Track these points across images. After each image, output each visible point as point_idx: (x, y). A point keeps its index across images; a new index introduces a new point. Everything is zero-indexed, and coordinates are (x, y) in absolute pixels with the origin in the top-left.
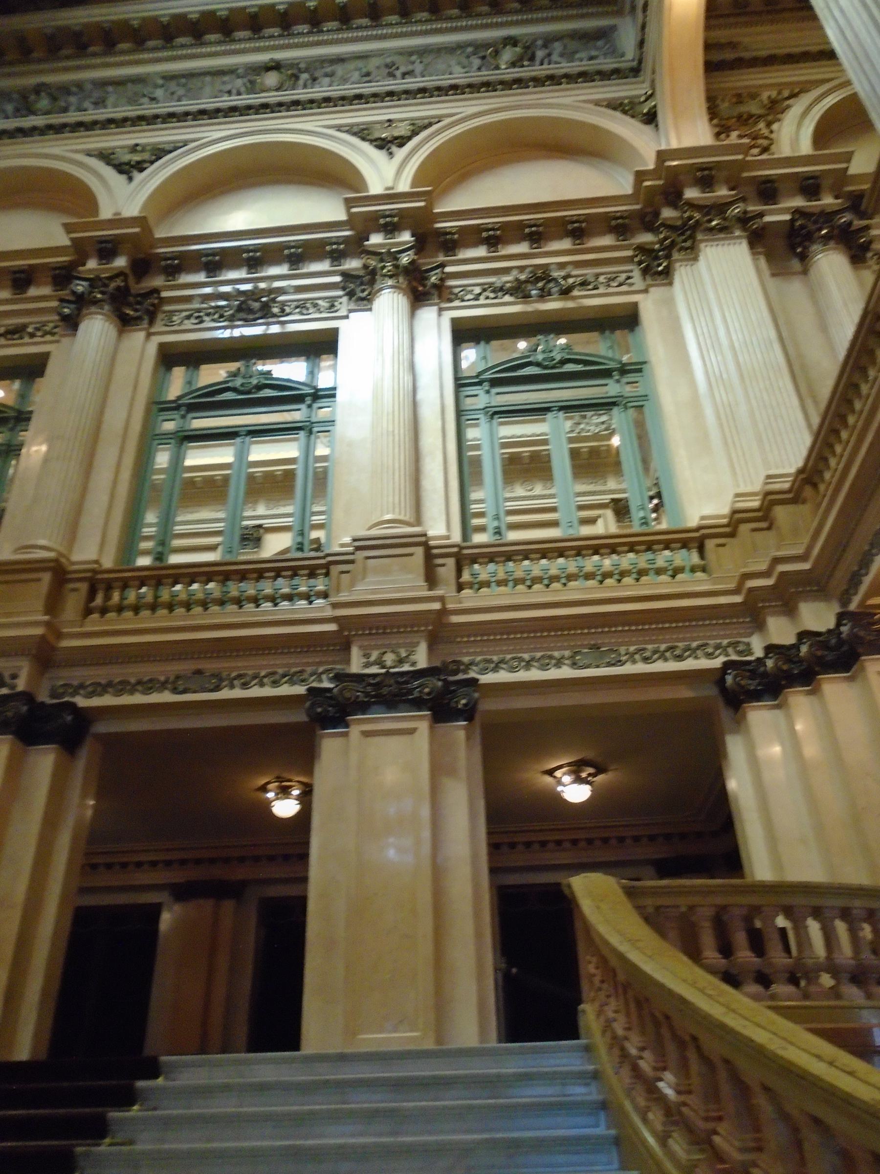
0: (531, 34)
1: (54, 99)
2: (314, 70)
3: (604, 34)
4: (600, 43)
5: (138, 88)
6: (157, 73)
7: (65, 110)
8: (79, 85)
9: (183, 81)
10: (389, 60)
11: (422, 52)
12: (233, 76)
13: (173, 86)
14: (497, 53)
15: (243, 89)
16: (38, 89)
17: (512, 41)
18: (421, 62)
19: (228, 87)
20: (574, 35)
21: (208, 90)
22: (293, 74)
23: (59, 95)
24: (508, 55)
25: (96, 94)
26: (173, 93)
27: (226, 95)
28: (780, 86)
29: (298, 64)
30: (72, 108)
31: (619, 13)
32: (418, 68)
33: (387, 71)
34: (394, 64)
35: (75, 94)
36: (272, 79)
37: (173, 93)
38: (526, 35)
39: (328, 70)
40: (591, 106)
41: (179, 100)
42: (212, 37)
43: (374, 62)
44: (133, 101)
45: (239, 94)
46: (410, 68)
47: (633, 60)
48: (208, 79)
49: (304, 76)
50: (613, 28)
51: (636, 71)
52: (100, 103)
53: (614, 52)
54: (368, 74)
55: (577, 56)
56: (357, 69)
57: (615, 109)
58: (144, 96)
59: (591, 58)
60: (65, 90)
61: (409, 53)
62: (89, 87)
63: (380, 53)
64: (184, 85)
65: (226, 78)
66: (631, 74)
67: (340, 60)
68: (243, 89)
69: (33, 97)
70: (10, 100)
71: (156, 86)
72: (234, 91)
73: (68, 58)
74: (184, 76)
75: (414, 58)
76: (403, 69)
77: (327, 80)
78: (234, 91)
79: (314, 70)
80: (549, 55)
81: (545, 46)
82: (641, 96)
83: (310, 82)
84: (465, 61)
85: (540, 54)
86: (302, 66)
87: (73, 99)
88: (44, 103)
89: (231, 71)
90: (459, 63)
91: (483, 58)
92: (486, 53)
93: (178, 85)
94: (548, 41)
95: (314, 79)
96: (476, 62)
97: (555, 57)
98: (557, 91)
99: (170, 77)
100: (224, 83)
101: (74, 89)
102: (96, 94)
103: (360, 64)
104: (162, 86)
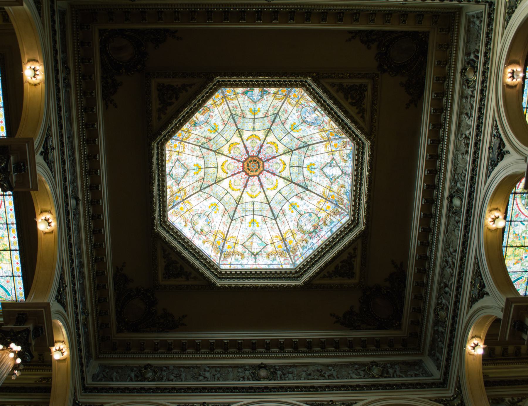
0: (383, 361)
1: (155, 373)
2: (285, 371)
3: (418, 364)
4: (416, 367)
5: (196, 370)
6: (206, 365)
7: (160, 379)
8: (167, 367)
9: (219, 369)
10: (319, 368)
11: (334, 365)
12: (243, 369)
13: (213, 371)
14: (369, 369)
15: (250, 377)
16: (147, 367)
17: (376, 364)
18: (334, 370)
19: (242, 375)
20: (404, 363)
21: (231, 375)
22: (274, 372)
23: (158, 372)
24: (376, 371)
25: (176, 372)
26: (214, 375)
27: (242, 379)
28: (512, 396)
29: (275, 366)
30: (165, 378)
31: (422, 354)
32: (335, 374)
33: (319, 373)
34: (322, 371)
35: (165, 371)
36: (263, 373)
37: (214, 375)
38: (382, 361)
39: (290, 370)
40: (427, 400)
41: (218, 380)
42: (233, 350)
43: (311, 368)
44: (196, 379)
45: (249, 379)
46: (330, 372)
47: (440, 379)
48: (230, 369)
49: (279, 373)
50: (421, 361)
51: (443, 384)
52: (178, 377)
53: (426, 373)
54: (310, 374)
55: (409, 373)
56: (303, 371)
57: (440, 403)
58: (200, 375)
59: (416, 375)
60: (161, 368)
61: (327, 365)
62: (171, 368)
63: (314, 364)
64: (219, 372)
65: (240, 370)
66: (441, 386)
67: (294, 366)
68: (250, 377)
69: (144, 371)
70: (132, 371)
71: (205, 371)
72: (246, 377)
73: (162, 353)
74: (218, 367)
75: (330, 368)
76: (327, 374)
77: (290, 376)
78: (246, 377)
79: (285, 371)
80: (395, 371)
81: (391, 367)
82: (450, 397)
83: (283, 376)
84: (356, 371)
85: (391, 371)
86: (277, 367)
87: (164, 374)
88: (150, 375)
89: (242, 367)
90: (353, 373)
91: (364, 371)
92: (366, 369)
93: (216, 371)
94: (393, 364)
95: (284, 375)
96: (362, 373)
97: (398, 373)
98: (407, 391)
99: (211, 367)
100: (238, 372)
101: (165, 368)
102: (176, 372)
103: (305, 369)
104: (209, 371)
